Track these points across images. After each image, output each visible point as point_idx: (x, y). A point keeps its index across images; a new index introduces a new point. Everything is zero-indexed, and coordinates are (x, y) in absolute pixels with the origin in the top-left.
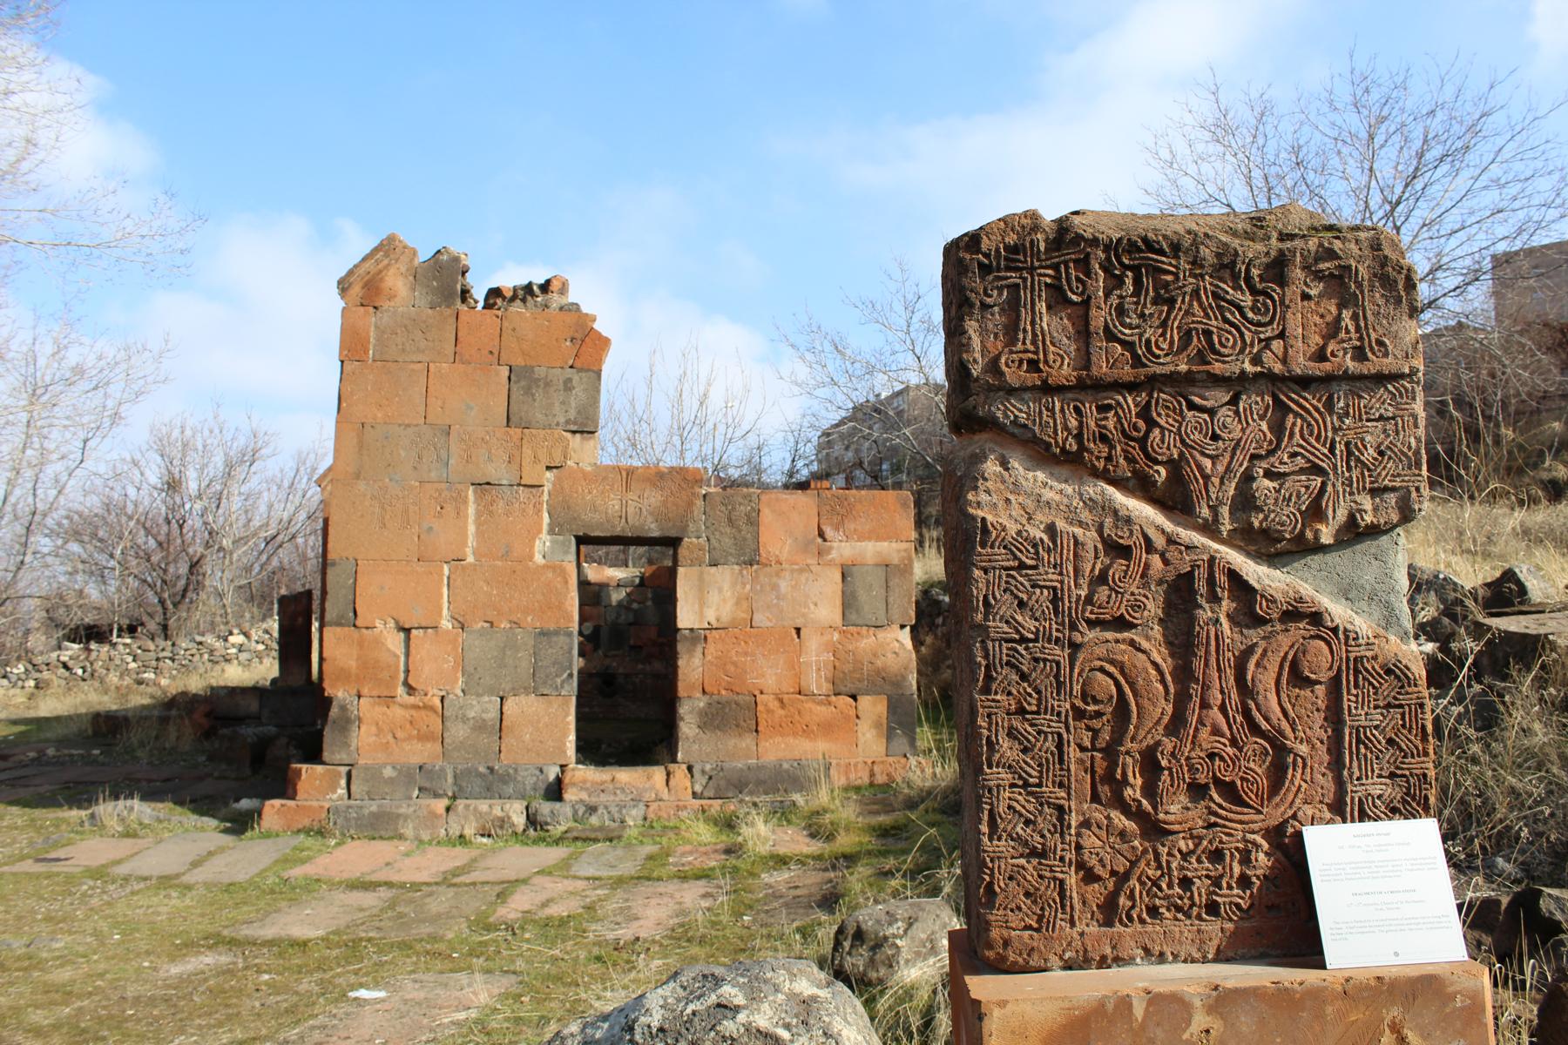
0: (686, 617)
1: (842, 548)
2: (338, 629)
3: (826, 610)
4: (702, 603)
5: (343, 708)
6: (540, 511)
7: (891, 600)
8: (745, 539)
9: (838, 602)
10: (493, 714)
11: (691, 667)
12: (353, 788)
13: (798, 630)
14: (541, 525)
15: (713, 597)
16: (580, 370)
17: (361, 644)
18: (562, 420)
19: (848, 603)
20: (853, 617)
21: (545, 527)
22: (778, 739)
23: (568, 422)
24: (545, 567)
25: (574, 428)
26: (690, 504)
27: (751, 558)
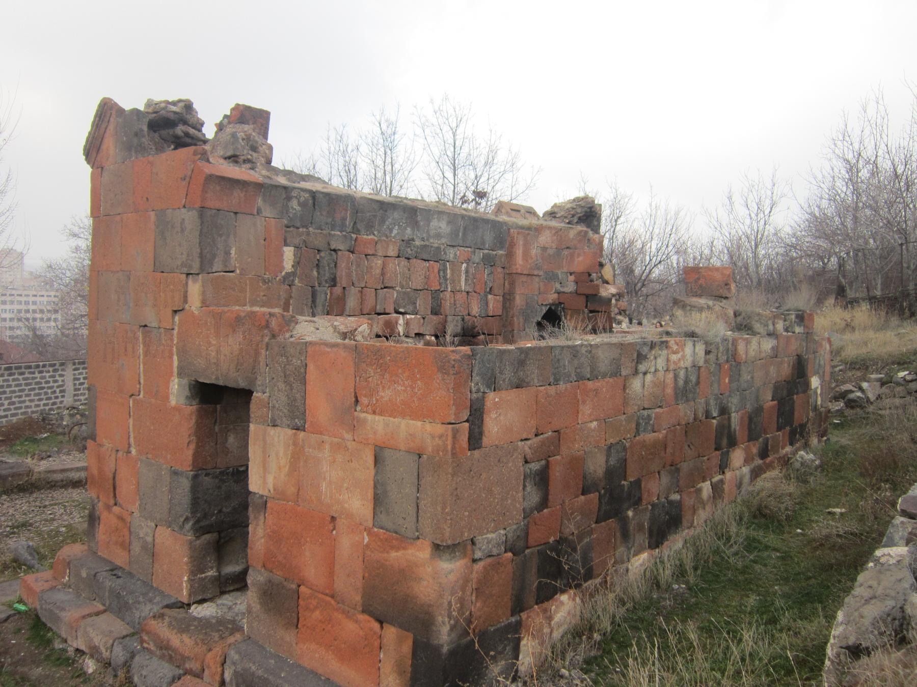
1: (377, 425)
6: (172, 355)
7: (422, 504)
8: (295, 400)
9: (370, 494)
10: (149, 539)
15: (273, 465)
18: (179, 263)
19: (379, 500)
20: (383, 517)
21: (175, 370)
22: (313, 646)
24: (176, 409)
26: (257, 354)
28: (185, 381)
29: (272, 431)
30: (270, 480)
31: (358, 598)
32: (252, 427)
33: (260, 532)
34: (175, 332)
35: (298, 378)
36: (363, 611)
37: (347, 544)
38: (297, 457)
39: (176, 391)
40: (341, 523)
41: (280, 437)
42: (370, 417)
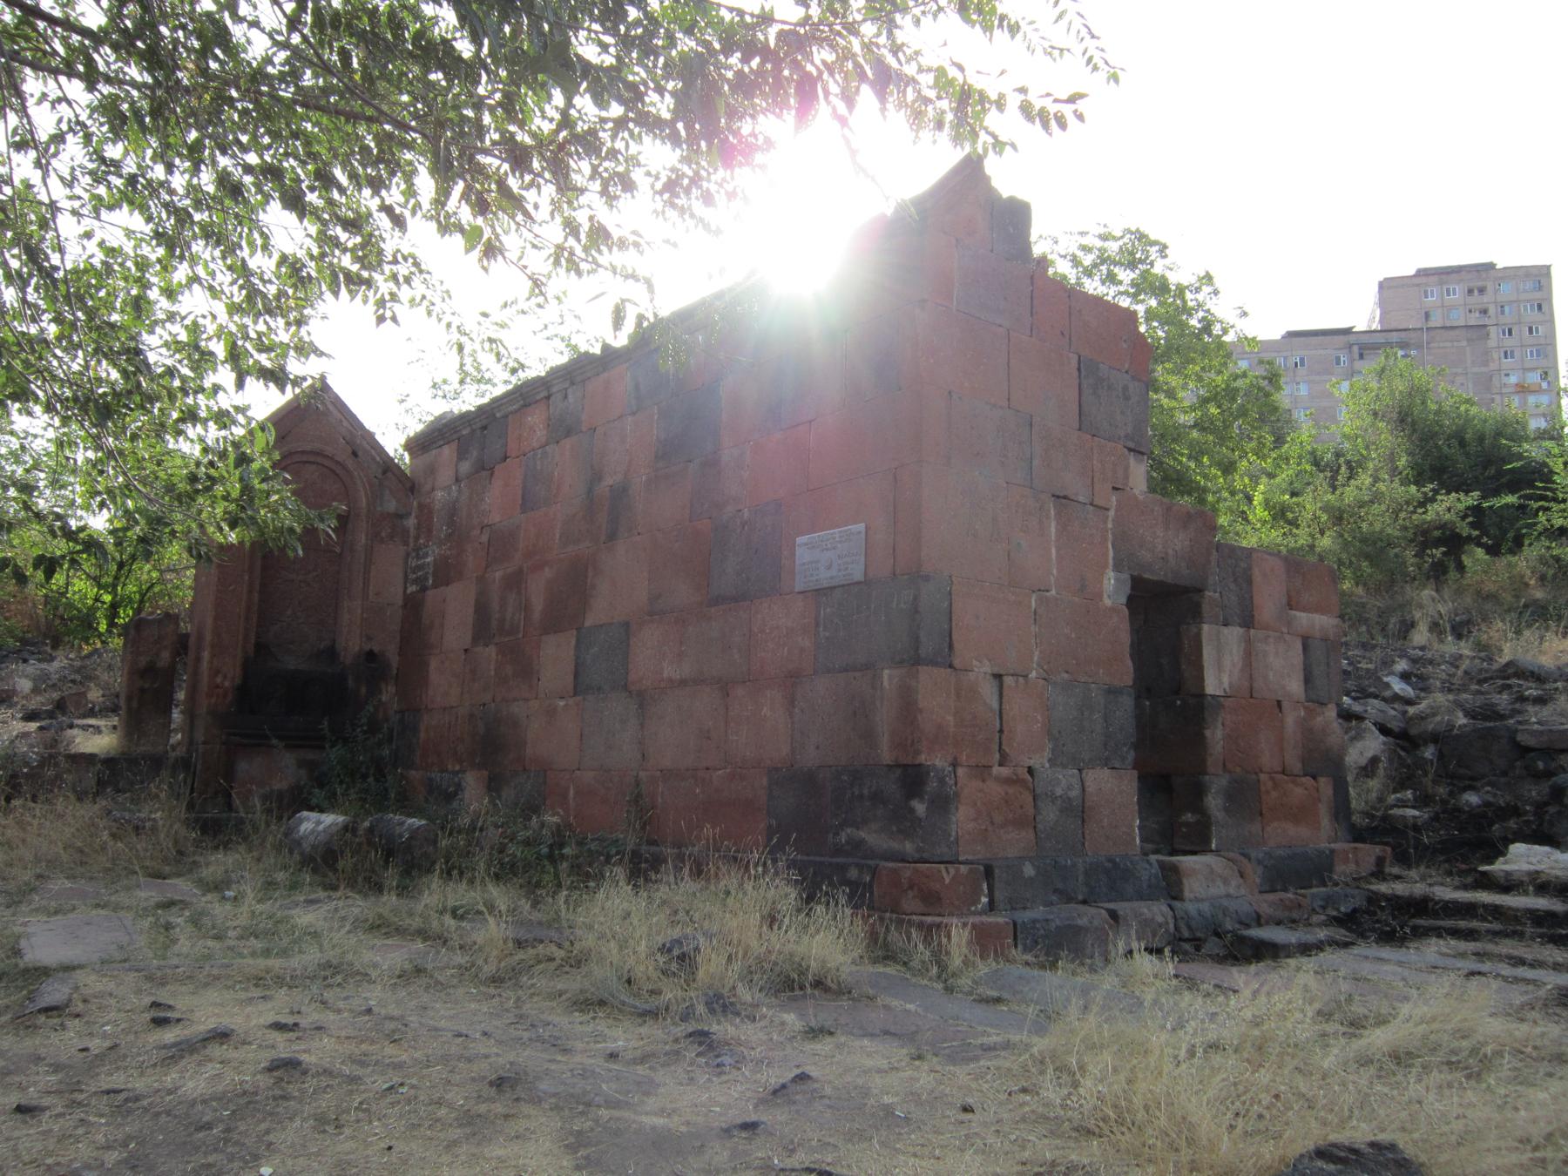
0: (1212, 686)
2: (935, 670)
3: (1295, 686)
4: (1220, 668)
5: (942, 781)
10: (1075, 793)
11: (1216, 735)
12: (998, 895)
13: (1279, 703)
14: (1106, 554)
15: (1227, 662)
16: (1133, 378)
17: (958, 695)
19: (1308, 680)
22: (1275, 824)
23: (1126, 436)
24: (1113, 609)
25: (1131, 445)
27: (1248, 621)
28: (1126, 576)
29: (1225, 630)
30: (1226, 680)
31: (1299, 765)
32: (1205, 627)
33: (1219, 733)
34: (1112, 513)
35: (1244, 580)
36: (1305, 775)
37: (1291, 719)
38: (1248, 654)
39: (1112, 587)
40: (1285, 705)
41: (1233, 634)
42: (1298, 614)
